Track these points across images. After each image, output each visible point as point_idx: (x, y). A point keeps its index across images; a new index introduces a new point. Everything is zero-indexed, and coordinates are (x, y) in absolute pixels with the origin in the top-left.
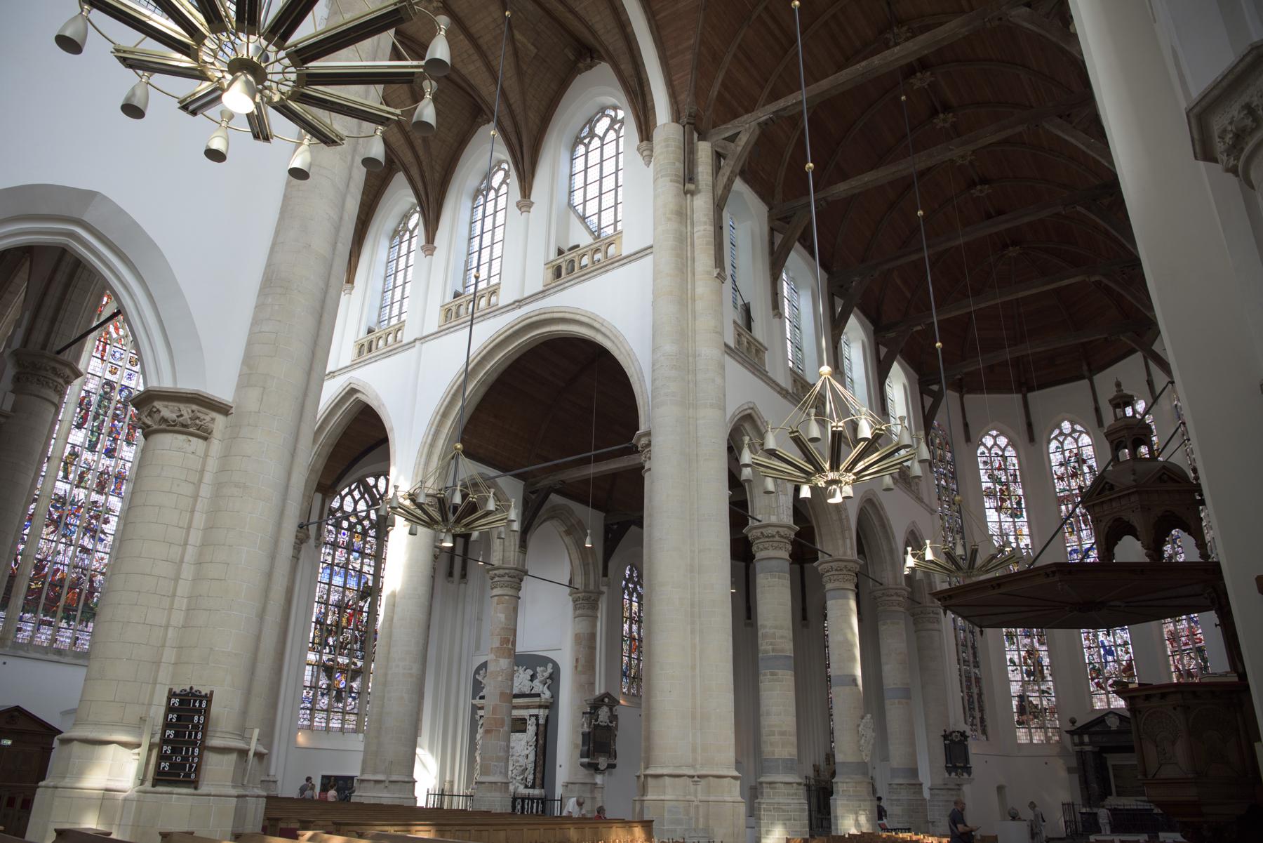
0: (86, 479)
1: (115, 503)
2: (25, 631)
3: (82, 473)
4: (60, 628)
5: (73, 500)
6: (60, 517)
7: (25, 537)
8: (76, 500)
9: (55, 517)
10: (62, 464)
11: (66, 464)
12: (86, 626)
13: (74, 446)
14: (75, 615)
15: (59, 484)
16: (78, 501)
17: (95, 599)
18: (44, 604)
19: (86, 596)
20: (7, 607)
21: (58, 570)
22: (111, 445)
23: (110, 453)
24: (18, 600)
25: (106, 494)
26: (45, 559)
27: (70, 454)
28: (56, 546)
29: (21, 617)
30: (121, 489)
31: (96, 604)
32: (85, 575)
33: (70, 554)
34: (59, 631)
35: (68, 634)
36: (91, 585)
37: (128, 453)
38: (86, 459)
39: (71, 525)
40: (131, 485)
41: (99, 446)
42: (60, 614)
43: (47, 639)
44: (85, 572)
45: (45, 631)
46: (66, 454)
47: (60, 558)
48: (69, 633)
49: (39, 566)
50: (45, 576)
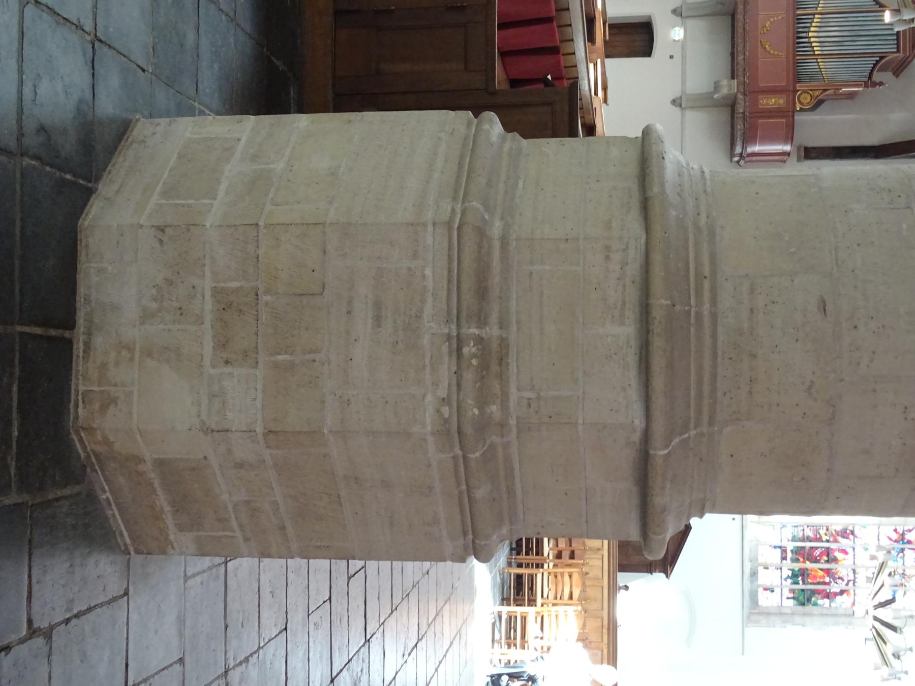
12: (788, 598)
14: (797, 583)
17: (820, 602)
18: (803, 548)
26: (855, 536)
31: (816, 604)
32: (847, 584)
36: (836, 594)
42: (797, 566)
44: (851, 584)
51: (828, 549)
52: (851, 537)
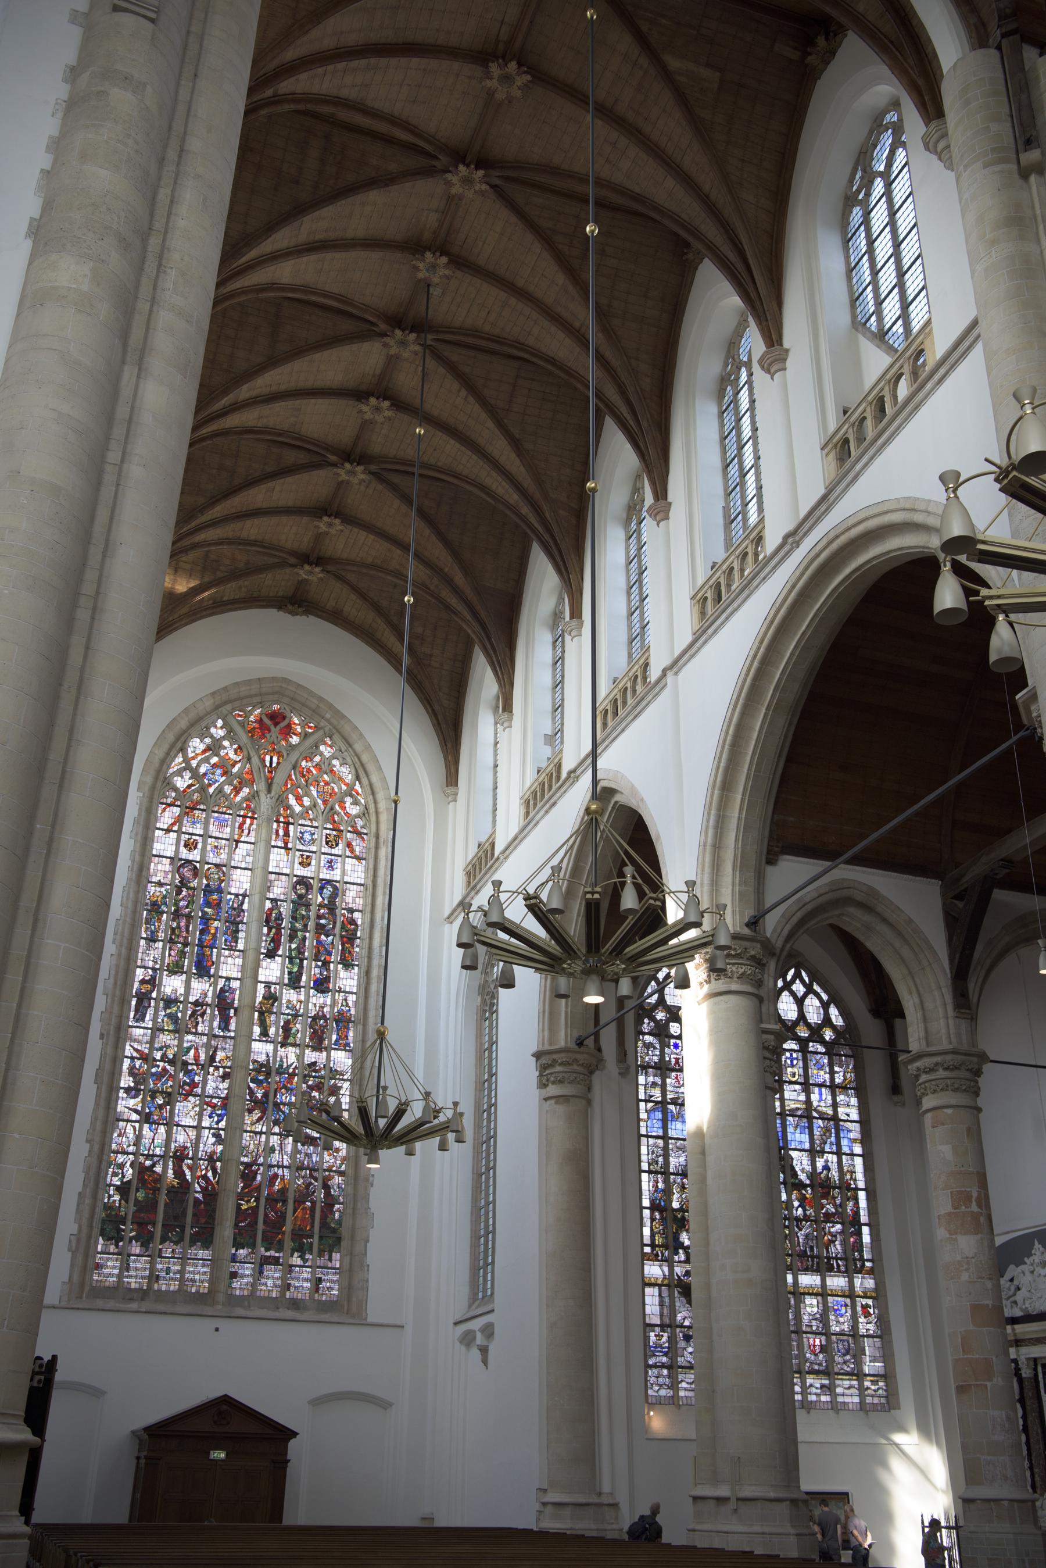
0: (294, 1030)
1: (342, 1060)
2: (243, 1276)
3: (287, 1023)
4: (291, 1266)
5: (281, 1066)
6: (266, 1095)
7: (222, 1132)
8: (285, 1065)
9: (259, 1096)
10: (256, 1014)
11: (261, 1013)
12: (330, 1259)
13: (268, 985)
14: (311, 1244)
15: (256, 1046)
16: (288, 1067)
17: (337, 1215)
18: (264, 1232)
19: (322, 1211)
20: (211, 1242)
21: (276, 1176)
22: (321, 974)
23: (322, 985)
24: (226, 1231)
25: (326, 1049)
26: (254, 1162)
27: (264, 997)
28: (267, 1140)
29: (234, 1255)
30: (347, 1037)
31: (339, 1222)
32: (316, 1180)
33: (289, 1149)
34: (290, 1272)
35: (305, 1275)
36: (328, 1194)
37: (348, 980)
38: (289, 1001)
39: (284, 1104)
40: (360, 1028)
41: (304, 978)
42: (288, 1244)
43: (275, 1285)
44: (315, 1174)
45: (271, 1274)
46: (259, 998)
47: (275, 1158)
48: (306, 1273)
49: (248, 1174)
50: (258, 1188)
51: (267, 1199)
52: (255, 1168)
